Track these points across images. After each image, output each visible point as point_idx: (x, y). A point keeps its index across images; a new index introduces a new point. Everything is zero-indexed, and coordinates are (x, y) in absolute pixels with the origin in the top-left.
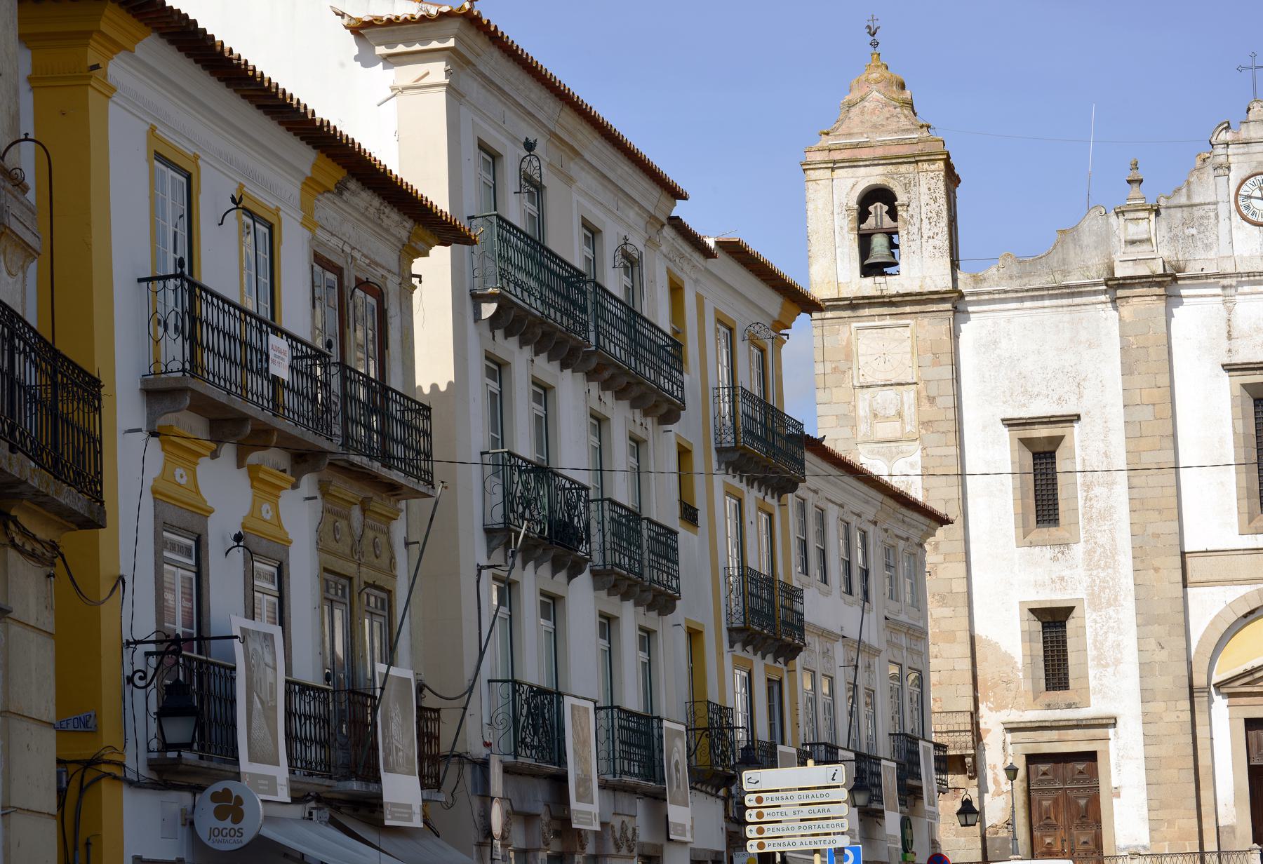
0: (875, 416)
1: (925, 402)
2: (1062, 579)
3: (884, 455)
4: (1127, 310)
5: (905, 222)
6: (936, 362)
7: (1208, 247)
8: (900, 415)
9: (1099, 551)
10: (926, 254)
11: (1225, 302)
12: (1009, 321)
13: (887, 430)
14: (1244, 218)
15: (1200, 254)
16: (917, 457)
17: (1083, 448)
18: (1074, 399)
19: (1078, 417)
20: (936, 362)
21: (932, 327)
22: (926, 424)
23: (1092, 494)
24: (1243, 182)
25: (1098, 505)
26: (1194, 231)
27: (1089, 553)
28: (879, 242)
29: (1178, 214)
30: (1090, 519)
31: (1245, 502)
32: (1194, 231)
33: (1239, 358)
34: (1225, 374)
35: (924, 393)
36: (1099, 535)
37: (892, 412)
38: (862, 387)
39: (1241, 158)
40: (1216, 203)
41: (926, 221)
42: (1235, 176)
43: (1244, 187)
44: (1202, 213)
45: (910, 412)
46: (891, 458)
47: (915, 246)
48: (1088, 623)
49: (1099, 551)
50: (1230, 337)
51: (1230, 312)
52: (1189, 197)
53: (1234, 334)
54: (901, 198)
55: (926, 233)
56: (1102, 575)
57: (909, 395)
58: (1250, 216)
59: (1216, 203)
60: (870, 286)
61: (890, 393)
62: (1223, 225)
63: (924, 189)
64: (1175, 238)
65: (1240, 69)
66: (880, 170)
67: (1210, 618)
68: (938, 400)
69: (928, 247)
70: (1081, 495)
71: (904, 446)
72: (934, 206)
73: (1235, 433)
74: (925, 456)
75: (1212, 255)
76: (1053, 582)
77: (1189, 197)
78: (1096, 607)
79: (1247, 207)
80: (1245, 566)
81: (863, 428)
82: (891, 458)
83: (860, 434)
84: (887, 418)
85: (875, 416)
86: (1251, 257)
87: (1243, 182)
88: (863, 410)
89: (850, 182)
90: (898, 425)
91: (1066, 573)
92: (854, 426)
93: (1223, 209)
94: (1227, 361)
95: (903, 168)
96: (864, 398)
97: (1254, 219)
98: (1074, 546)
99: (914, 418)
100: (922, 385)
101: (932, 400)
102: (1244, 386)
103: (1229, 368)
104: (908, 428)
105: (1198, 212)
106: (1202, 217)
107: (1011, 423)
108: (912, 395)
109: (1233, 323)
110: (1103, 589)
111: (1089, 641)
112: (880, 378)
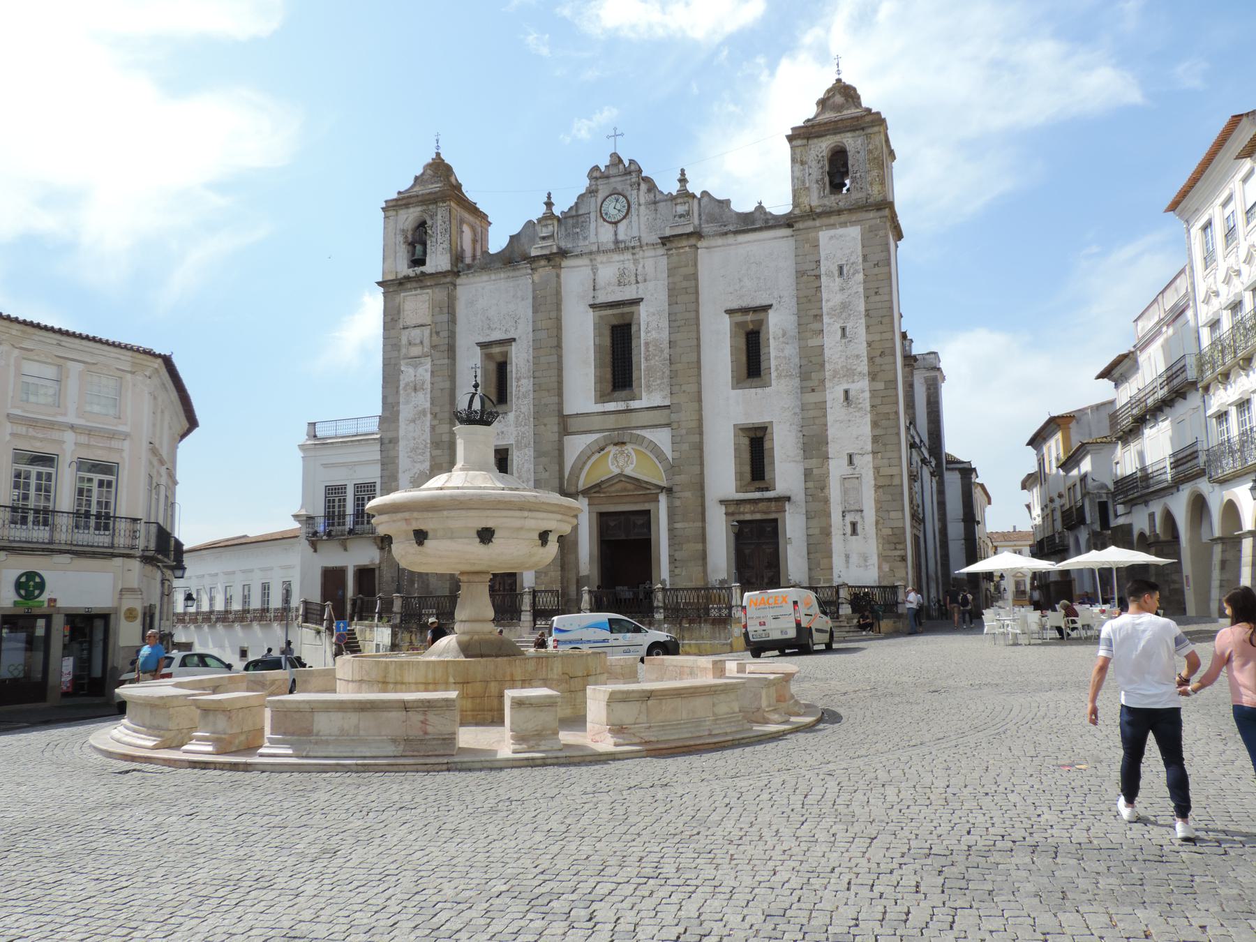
0: (410, 344)
1: (434, 335)
2: (502, 433)
3: (412, 366)
4: (536, 277)
5: (431, 236)
6: (441, 312)
7: (585, 238)
8: (422, 343)
9: (522, 416)
10: (439, 253)
11: (592, 269)
12: (483, 289)
13: (415, 351)
14: (604, 220)
15: (581, 243)
16: (429, 366)
17: (517, 358)
18: (513, 329)
19: (514, 340)
20: (441, 312)
21: (440, 294)
22: (433, 347)
23: (520, 383)
24: (604, 200)
25: (523, 390)
26: (578, 230)
27: (517, 417)
28: (419, 248)
29: (570, 221)
30: (518, 398)
31: (598, 385)
32: (578, 230)
33: (598, 301)
34: (591, 310)
35: (434, 330)
36: (522, 407)
37: (418, 341)
38: (404, 328)
39: (605, 186)
40: (589, 213)
41: (439, 234)
42: (601, 196)
43: (605, 203)
44: (583, 219)
45: (427, 342)
46: (416, 367)
47: (434, 249)
48: (515, 458)
49: (522, 416)
50: (594, 290)
51: (595, 274)
52: (577, 211)
53: (597, 287)
54: (429, 223)
55: (439, 241)
56: (523, 430)
57: (427, 331)
58: (607, 219)
59: (589, 213)
60: (410, 272)
61: (417, 331)
62: (593, 225)
63: (439, 217)
64: (568, 235)
65: (608, 137)
66: (419, 209)
67: (577, 453)
68: (441, 334)
69: (440, 249)
70: (514, 384)
71: (422, 360)
72: (444, 226)
73: (595, 344)
74: (433, 365)
75: (587, 243)
76: (498, 434)
77: (577, 211)
78: (519, 449)
79: (606, 214)
80: (597, 422)
81: (404, 351)
82: (416, 367)
83: (402, 354)
84: (415, 344)
85: (410, 344)
86: (607, 242)
87: (604, 200)
88: (404, 341)
89: (405, 216)
90: (420, 348)
91: (505, 429)
92: (399, 351)
93: (593, 216)
94: (592, 302)
95: (431, 207)
96: (406, 332)
97: (610, 220)
98: (510, 414)
99: (429, 344)
100: (433, 325)
101: (438, 333)
102: (600, 317)
103: (592, 306)
104: (425, 350)
105: (581, 219)
106: (583, 222)
107: (483, 345)
108: (428, 331)
109: (597, 281)
110: (523, 438)
111: (515, 468)
112: (414, 322)
